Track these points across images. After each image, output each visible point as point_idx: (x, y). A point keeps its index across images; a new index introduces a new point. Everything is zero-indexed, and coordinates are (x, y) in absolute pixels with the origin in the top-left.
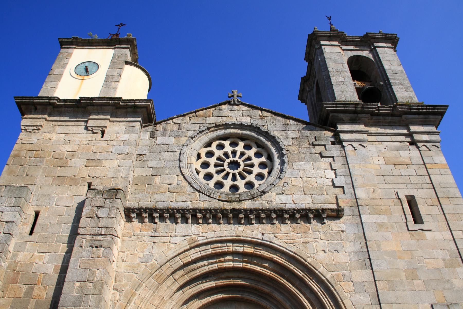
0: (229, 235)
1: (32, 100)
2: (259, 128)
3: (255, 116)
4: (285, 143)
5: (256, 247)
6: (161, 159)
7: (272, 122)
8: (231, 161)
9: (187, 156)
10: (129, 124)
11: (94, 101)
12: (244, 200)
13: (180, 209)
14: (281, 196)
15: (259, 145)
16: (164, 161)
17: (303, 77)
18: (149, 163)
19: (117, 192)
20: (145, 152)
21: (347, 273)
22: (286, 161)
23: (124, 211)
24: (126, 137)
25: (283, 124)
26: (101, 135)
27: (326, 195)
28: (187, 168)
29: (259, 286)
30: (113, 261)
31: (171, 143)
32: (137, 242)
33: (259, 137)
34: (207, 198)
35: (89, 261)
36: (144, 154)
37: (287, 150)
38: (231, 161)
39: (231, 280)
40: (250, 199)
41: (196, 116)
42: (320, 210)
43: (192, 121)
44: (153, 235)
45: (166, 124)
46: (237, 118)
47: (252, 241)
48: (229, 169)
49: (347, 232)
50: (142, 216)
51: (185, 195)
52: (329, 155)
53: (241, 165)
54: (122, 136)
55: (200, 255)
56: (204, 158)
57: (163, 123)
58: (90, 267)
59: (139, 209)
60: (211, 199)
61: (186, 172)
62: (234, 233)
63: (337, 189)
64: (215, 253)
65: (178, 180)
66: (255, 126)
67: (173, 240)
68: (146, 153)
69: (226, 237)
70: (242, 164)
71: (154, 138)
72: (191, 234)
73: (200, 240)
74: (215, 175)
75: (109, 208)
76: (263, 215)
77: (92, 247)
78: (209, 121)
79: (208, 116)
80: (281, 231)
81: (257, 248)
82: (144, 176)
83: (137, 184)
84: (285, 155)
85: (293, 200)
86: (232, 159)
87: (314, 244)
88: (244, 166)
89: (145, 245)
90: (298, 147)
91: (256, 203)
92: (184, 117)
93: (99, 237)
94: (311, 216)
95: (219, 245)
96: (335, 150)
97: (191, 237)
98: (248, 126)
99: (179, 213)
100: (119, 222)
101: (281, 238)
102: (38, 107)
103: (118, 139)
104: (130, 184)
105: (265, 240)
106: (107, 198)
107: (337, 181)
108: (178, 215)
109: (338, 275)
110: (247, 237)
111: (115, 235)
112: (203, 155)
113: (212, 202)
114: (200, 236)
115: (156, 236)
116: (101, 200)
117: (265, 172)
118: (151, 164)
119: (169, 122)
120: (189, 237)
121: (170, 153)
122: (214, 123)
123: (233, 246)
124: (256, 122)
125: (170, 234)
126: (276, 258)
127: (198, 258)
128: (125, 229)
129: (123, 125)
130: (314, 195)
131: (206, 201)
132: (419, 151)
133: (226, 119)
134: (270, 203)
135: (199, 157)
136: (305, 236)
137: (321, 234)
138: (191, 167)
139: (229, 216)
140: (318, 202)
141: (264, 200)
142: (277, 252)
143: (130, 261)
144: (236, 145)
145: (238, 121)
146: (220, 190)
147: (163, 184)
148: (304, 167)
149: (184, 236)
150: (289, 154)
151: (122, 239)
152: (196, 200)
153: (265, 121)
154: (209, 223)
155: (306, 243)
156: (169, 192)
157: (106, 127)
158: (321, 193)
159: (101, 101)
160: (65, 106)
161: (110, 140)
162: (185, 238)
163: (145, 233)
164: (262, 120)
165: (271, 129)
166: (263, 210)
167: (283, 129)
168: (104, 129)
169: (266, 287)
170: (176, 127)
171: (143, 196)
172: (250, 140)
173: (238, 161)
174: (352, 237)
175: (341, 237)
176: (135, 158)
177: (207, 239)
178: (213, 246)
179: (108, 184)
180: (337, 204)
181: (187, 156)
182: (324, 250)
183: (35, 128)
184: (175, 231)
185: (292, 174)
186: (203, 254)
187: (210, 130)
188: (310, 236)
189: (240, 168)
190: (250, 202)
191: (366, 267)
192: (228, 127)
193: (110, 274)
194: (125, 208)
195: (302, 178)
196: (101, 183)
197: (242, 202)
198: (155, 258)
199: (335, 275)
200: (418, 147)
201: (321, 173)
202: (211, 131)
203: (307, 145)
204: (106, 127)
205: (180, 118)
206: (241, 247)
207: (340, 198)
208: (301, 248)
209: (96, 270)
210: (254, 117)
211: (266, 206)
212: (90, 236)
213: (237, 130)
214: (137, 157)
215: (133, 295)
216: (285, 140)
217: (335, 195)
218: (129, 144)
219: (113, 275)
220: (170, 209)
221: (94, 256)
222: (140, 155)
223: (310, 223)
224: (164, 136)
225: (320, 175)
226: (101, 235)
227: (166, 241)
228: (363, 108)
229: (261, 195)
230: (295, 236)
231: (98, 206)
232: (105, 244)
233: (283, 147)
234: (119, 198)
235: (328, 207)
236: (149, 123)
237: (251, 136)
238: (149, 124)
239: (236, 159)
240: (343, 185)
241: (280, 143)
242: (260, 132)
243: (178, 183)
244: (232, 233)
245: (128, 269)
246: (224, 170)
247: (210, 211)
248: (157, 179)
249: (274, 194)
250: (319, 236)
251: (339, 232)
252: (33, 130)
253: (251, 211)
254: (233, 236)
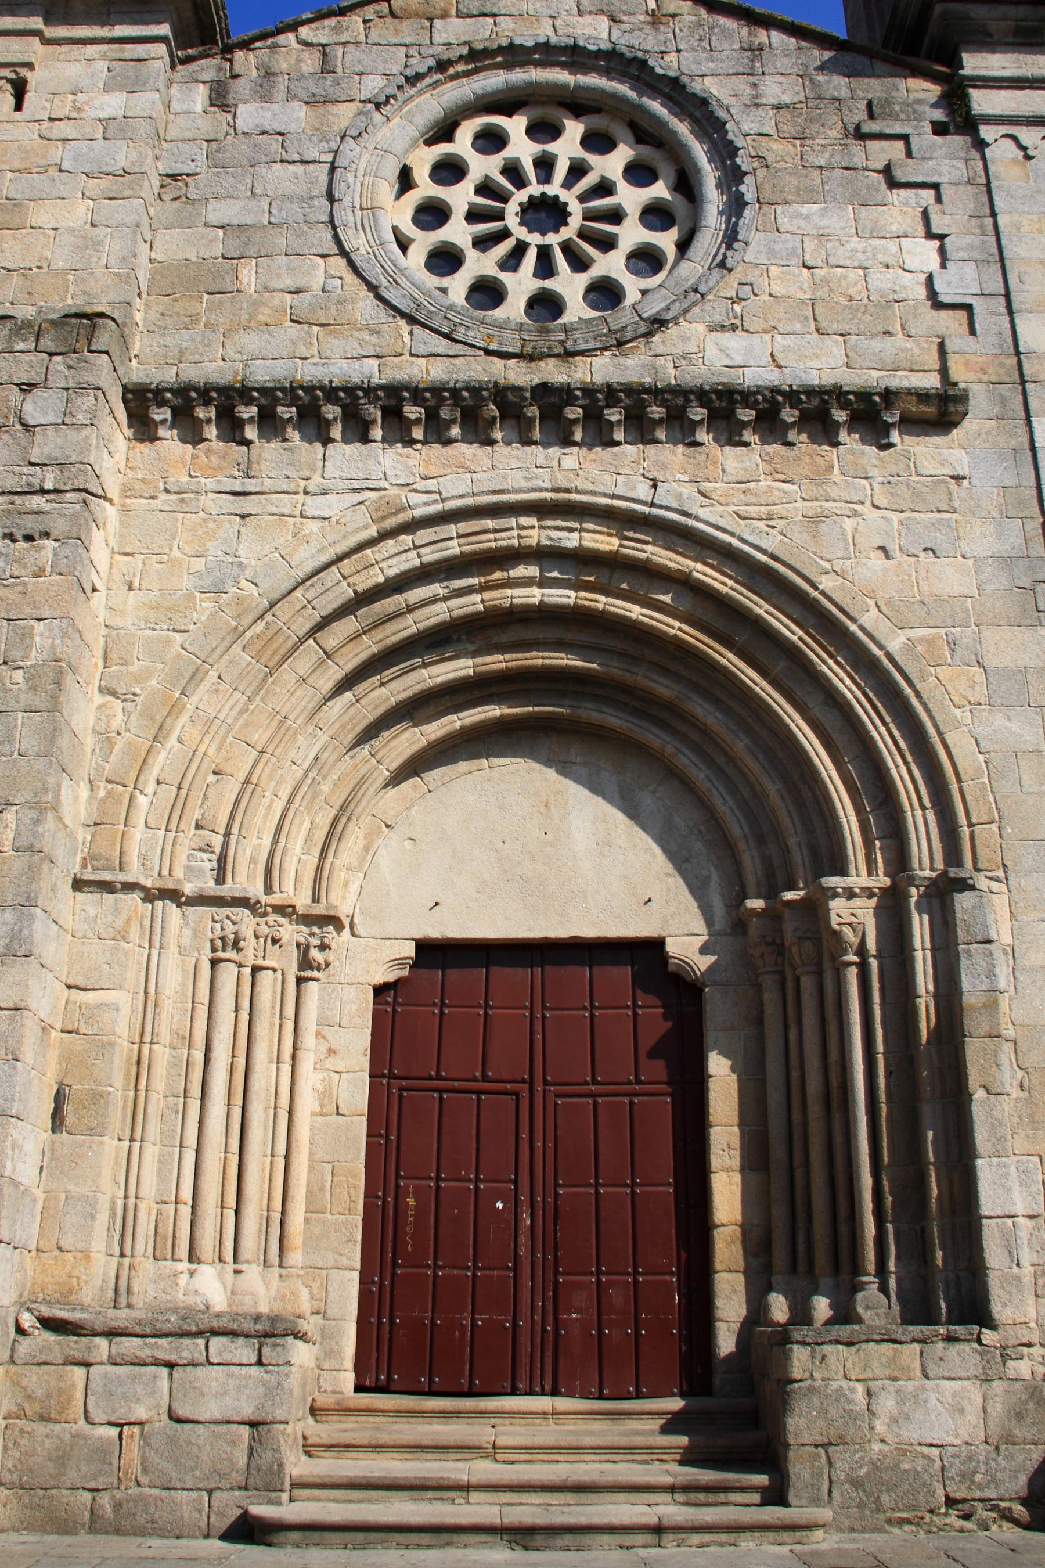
0: (524, 484)
2: (644, 62)
3: (630, 14)
4: (746, 127)
5: (626, 533)
6: (259, 191)
7: (697, 37)
8: (531, 197)
9: (360, 178)
10: (122, 51)
12: (582, 353)
13: (337, 389)
14: (727, 339)
15: (645, 132)
16: (268, 200)
18: (210, 208)
19: (94, 327)
20: (193, 164)
21: (965, 635)
22: (749, 196)
23: (125, 400)
24: (114, 104)
25: (743, 49)
26: (11, 101)
27: (900, 335)
28: (359, 227)
29: (636, 674)
30: (94, 590)
31: (293, 127)
32: (180, 516)
33: (645, 100)
34: (442, 345)
36: (188, 175)
37: (753, 154)
38: (531, 197)
39: (534, 653)
40: (606, 349)
41: (393, 14)
42: (875, 394)
43: (374, 36)
44: (238, 489)
45: (269, 47)
46: (558, 23)
47: (613, 507)
48: (524, 229)
49: (974, 482)
50: (192, 416)
51: (356, 334)
52: (920, 179)
53: (570, 214)
54: (97, 102)
55: (417, 562)
56: (426, 188)
58: (8, 611)
59: (183, 391)
60: (458, 348)
61: (357, 242)
62: (547, 477)
63: (944, 314)
64: (475, 553)
65: (328, 276)
66: (629, 55)
67: (315, 505)
68: (198, 170)
69: (516, 491)
70: (575, 208)
71: (227, 106)
72: (383, 484)
73: (417, 506)
74: (471, 255)
75: (67, 389)
76: (656, 412)
78: (444, 35)
79: (438, 13)
80: (723, 471)
81: (631, 534)
82: (194, 259)
83: (170, 291)
84: (746, 173)
85: (772, 355)
86: (535, 189)
87: (849, 524)
88: (584, 219)
89: (211, 525)
90: (798, 142)
91: (629, 362)
92: (345, 20)
93: (37, 502)
94: (841, 416)
95: (490, 524)
97: (383, 493)
98: (599, 54)
99: (336, 401)
100: (106, 442)
101: (722, 501)
103: (81, 115)
104: (139, 295)
105: (661, 507)
106: (53, 350)
107: (949, 283)
108: (331, 411)
109: (930, 642)
110: (593, 493)
111: (94, 490)
112: (422, 174)
113: (458, 361)
114: (416, 491)
115: (250, 493)
116: (34, 359)
117: (666, 241)
118: (221, 211)
119: (281, 39)
120: (373, 495)
121: (291, 167)
122: (465, 43)
123: (541, 527)
125: (303, 483)
126: (702, 572)
127: (410, 570)
128: (131, 468)
129: (96, 56)
130: (854, 338)
131: (439, 355)
133: (512, 26)
134: (684, 362)
135: (406, 181)
136: (815, 491)
137: (875, 485)
138: (375, 222)
139: (525, 415)
140: (870, 365)
141: (659, 351)
142: (708, 552)
143: (155, 586)
144: (554, 132)
145: (560, 32)
146: (490, 313)
147: (267, 289)
148: (822, 224)
149: (355, 490)
150: (761, 173)
151: (123, 506)
152: (399, 350)
153: (671, 36)
154: (448, 442)
155: (816, 520)
156: (292, 321)
157: (30, 66)
158: (880, 329)
161: (51, 119)
162: (359, 497)
163: (209, 483)
164: (657, 30)
165: (693, 67)
166: (656, 393)
167: (741, 70)
168: (24, 72)
169: (662, 680)
170: (310, 62)
171: (192, 340)
172: (607, 111)
173: (562, 199)
174: (991, 500)
175: (950, 500)
176: (156, 191)
177: (443, 500)
178: (464, 527)
179: (57, 298)
180: (944, 371)
181: (360, 178)
182: (882, 548)
184: (320, 472)
185: (771, 252)
186: (430, 555)
187: (446, 70)
188: (833, 492)
189: (566, 224)
190: (608, 360)
191: (1036, 614)
192: (522, 58)
193: (85, 635)
194: (126, 389)
195: (809, 268)
196: (29, 293)
197: (577, 358)
198: (249, 573)
199: (922, 640)
201: (885, 251)
202: (457, 76)
203: (834, 133)
204: (30, 66)
205: (326, 22)
206: (571, 530)
207: (957, 348)
208: (797, 538)
209: (32, 622)
210: (625, 18)
211: (670, 375)
213: (558, 70)
214: (162, 186)
215: (175, 709)
216: (748, 115)
217: (938, 336)
218: (129, 134)
219: (97, 640)
220: (302, 387)
221: (23, 573)
222: (174, 177)
223: (836, 444)
224: (266, 98)
225: (880, 257)
226: (43, 492)
227: (286, 511)
229: (649, 334)
230: (776, 493)
231: (23, 384)
232: (59, 526)
233: (739, 142)
234: (104, 349)
235: (906, 384)
236: (203, 44)
237: (614, 96)
238: (201, 49)
239: (554, 189)
240: (968, 300)
241: (728, 126)
242: (647, 78)
243: (329, 287)
244: (536, 477)
245: (152, 615)
246: (504, 234)
247: (455, 392)
248: (245, 272)
249: (701, 328)
250: (869, 492)
251: (943, 482)
253: (611, 393)
254: (541, 490)
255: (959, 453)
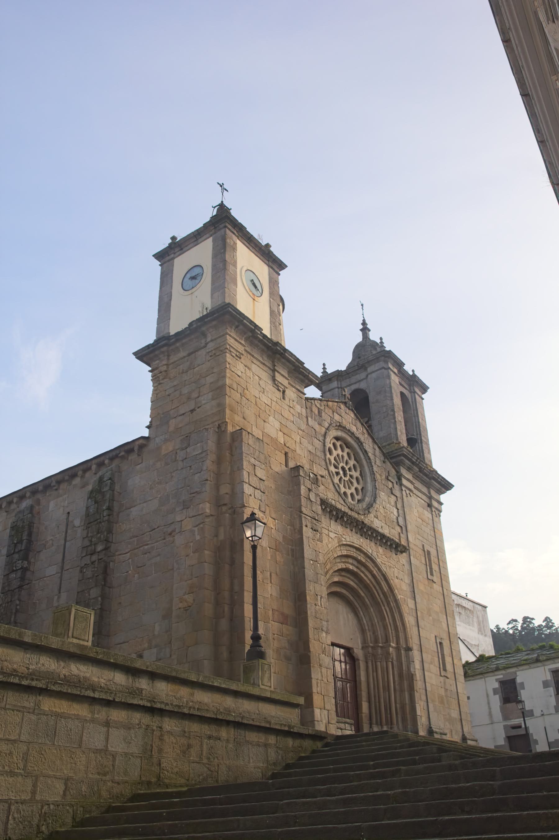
1: (242, 317)
11: (286, 354)
17: (340, 370)
35: (313, 542)
57: (309, 401)
60: (345, 504)
77: (312, 528)
87: (393, 569)
96: (397, 491)
102: (241, 327)
108: (335, 513)
124: (362, 439)
132: (432, 514)
157: (287, 388)
159: (290, 358)
160: (261, 341)
183: (238, 354)
188: (391, 562)
200: (432, 511)
212: (310, 518)
226: (315, 519)
228: (419, 463)
240: (402, 526)
246: (349, 479)
252: (236, 355)
255: (404, 560)
